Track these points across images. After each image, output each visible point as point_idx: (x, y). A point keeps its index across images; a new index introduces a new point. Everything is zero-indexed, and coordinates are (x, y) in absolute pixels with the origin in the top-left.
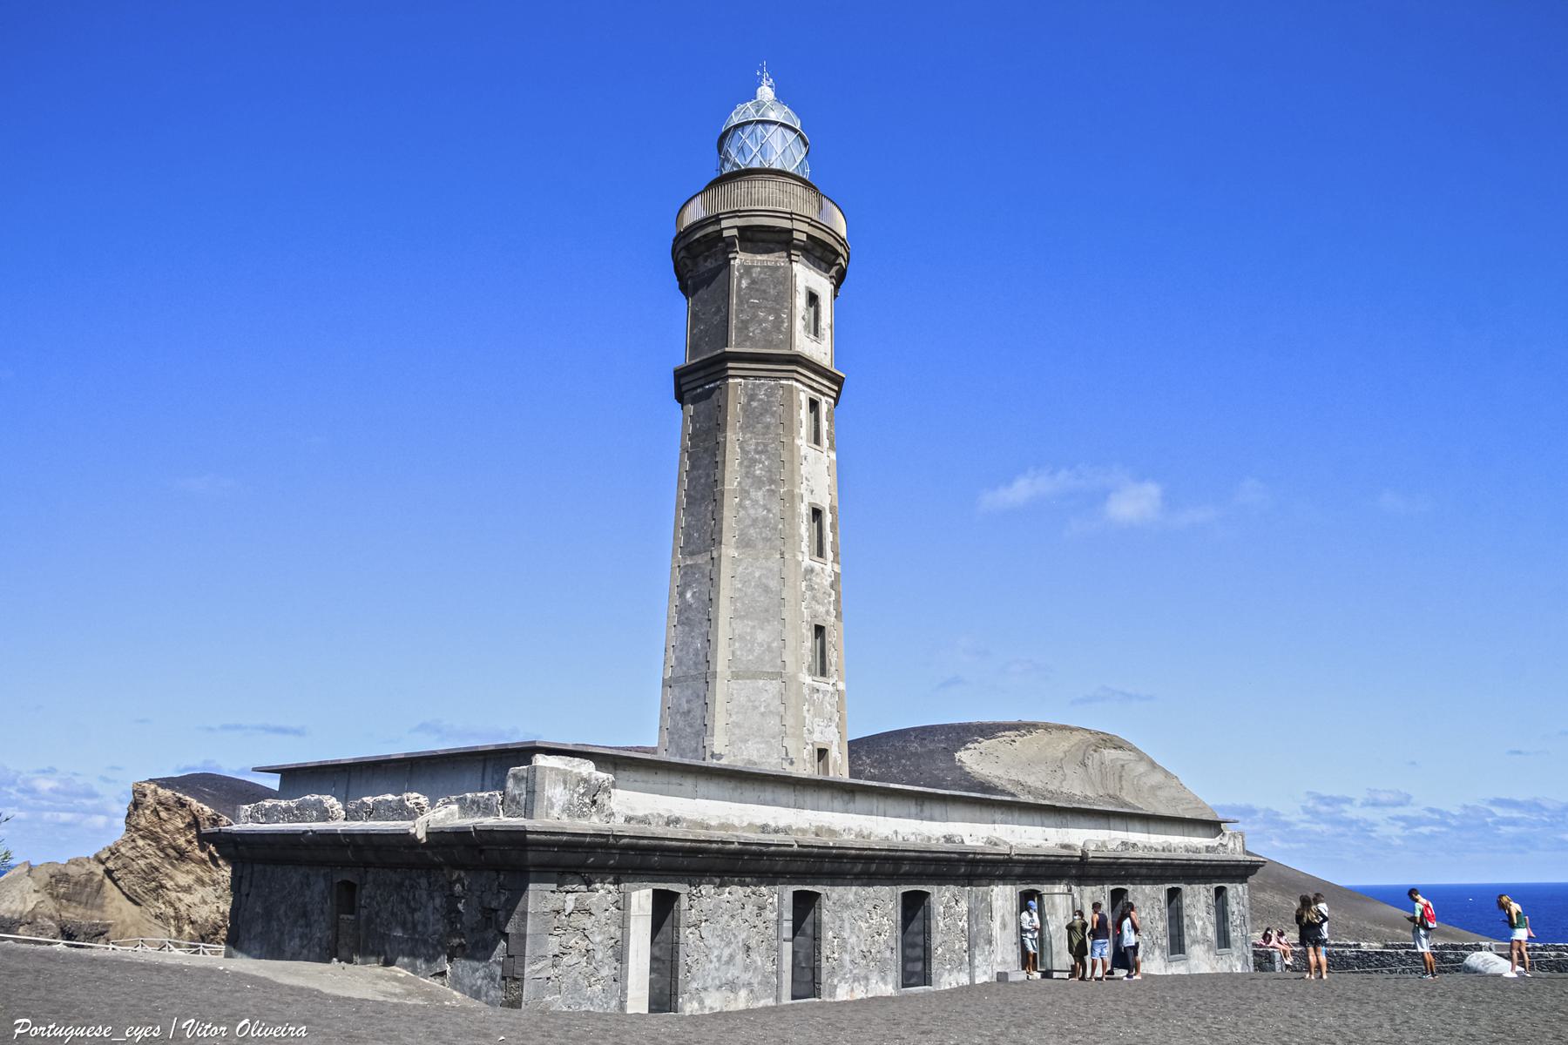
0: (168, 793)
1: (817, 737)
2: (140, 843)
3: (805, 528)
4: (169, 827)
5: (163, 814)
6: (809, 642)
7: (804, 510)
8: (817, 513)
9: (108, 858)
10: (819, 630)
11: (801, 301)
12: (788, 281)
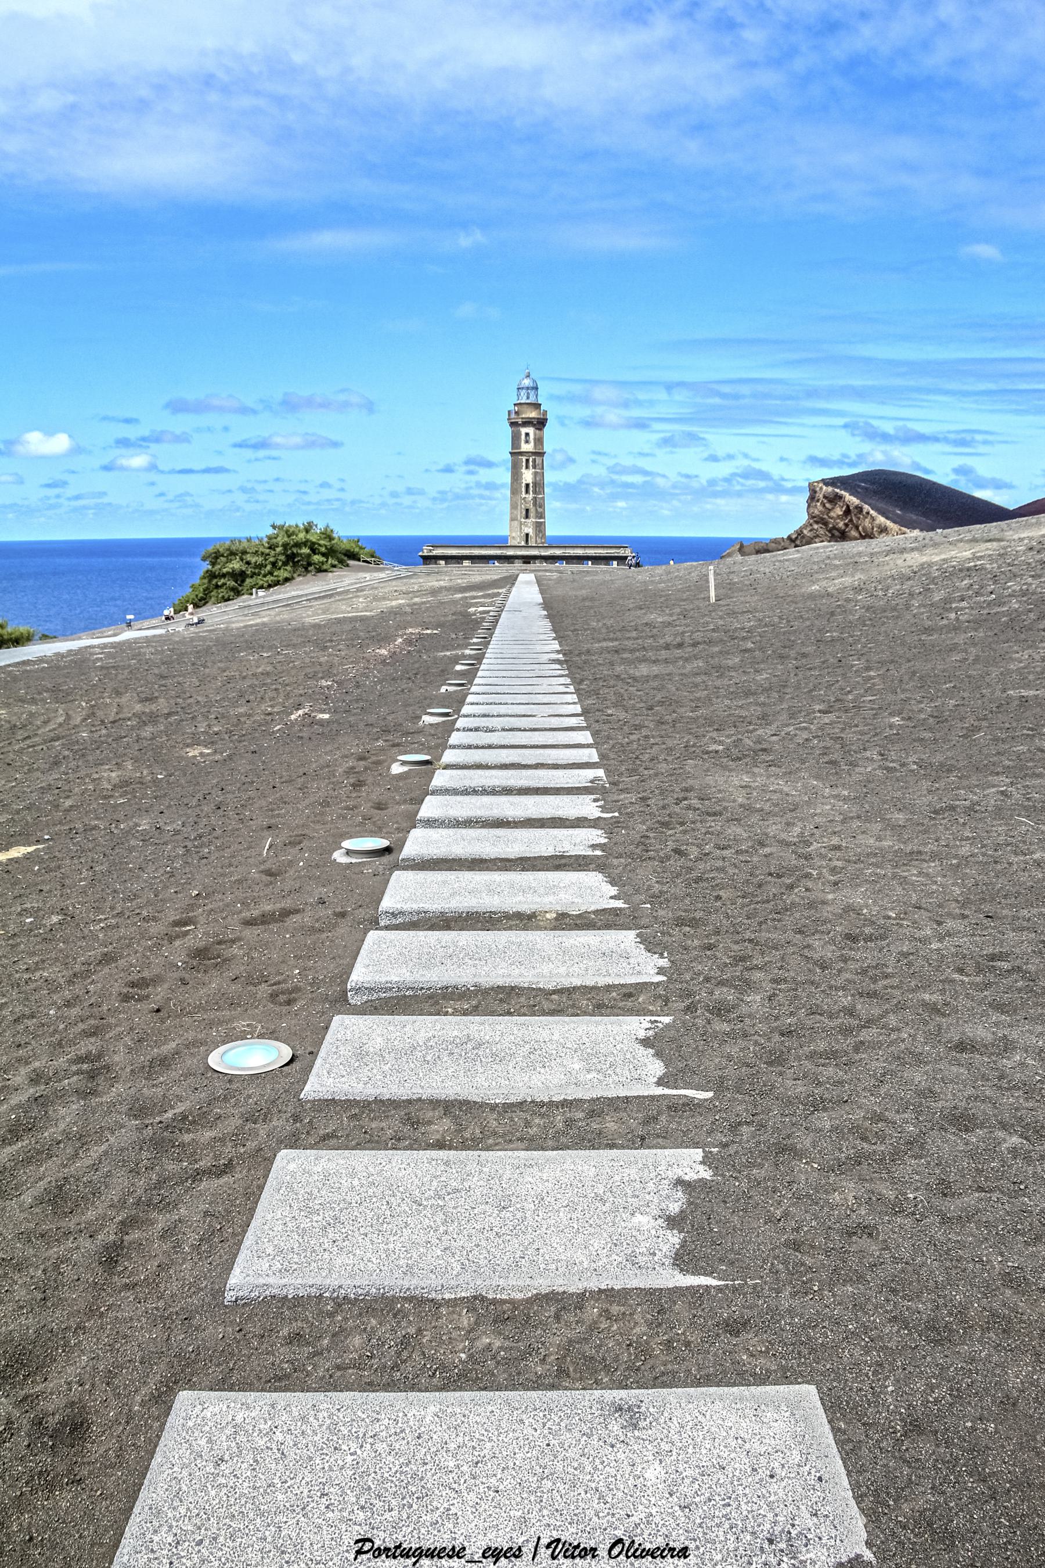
0: (830, 489)
1: (526, 531)
2: (816, 526)
3: (523, 489)
4: (832, 514)
5: (828, 505)
6: (524, 513)
7: (523, 485)
8: (527, 485)
9: (797, 538)
10: (527, 510)
11: (523, 437)
12: (520, 434)
